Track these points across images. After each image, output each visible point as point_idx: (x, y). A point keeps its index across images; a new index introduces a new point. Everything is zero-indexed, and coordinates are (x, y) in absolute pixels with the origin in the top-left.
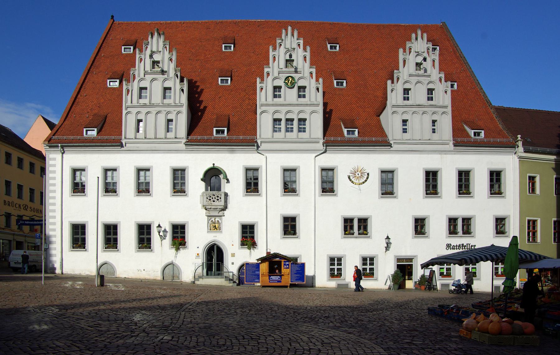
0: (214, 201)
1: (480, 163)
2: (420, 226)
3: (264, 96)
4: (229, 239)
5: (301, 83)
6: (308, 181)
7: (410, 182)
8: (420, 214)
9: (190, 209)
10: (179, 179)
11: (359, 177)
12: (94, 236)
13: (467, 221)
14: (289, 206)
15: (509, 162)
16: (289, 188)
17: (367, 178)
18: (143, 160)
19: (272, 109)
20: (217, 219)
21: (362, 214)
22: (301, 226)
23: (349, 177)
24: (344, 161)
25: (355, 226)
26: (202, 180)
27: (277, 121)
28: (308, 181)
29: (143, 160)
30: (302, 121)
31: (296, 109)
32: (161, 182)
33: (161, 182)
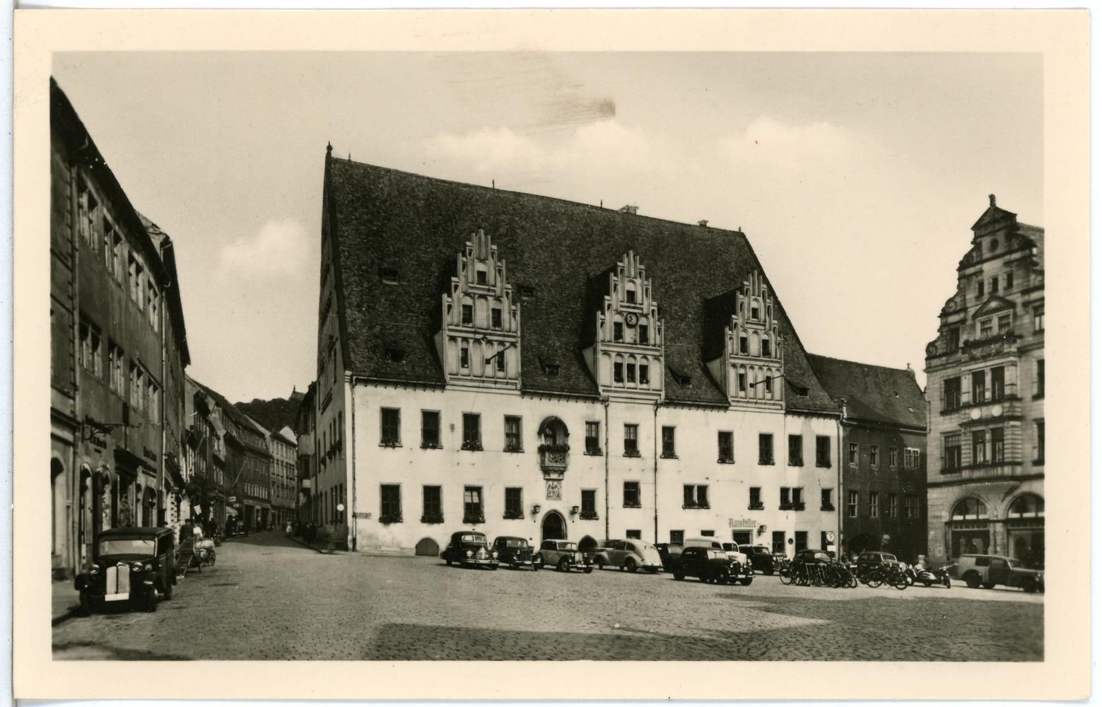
2: (755, 500)
5: (643, 321)
6: (649, 442)
7: (746, 448)
9: (524, 470)
16: (631, 448)
21: (702, 482)
22: (645, 495)
27: (618, 367)
28: (649, 442)
30: (644, 369)
33: (493, 433)
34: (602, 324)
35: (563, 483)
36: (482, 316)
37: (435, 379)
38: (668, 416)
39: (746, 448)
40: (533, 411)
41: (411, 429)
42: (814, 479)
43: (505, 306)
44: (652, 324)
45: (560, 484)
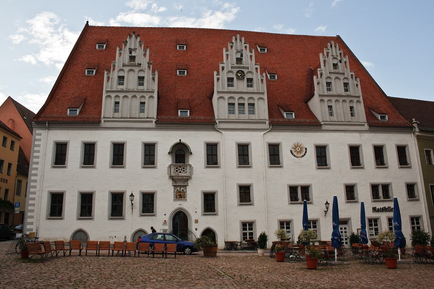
0: (180, 172)
1: (390, 141)
3: (220, 85)
4: (193, 205)
5: (249, 76)
6: (259, 154)
7: (339, 156)
8: (350, 182)
9: (158, 180)
10: (149, 152)
11: (298, 151)
12: (71, 205)
13: (386, 187)
14: (244, 177)
15: (410, 141)
17: (306, 152)
18: (118, 136)
19: (226, 96)
20: (182, 189)
22: (256, 194)
23: (291, 152)
24: (286, 139)
25: (300, 194)
26: (169, 153)
27: (231, 105)
28: (259, 154)
29: (118, 136)
31: (246, 97)
32: (134, 155)
33: (134, 155)
34: (218, 79)
35: (188, 188)
36: (131, 81)
37: (93, 122)
38: (275, 137)
39: (339, 156)
40: (166, 140)
41: (75, 154)
42: (396, 177)
43: (147, 74)
44: (257, 77)
45: (186, 189)
